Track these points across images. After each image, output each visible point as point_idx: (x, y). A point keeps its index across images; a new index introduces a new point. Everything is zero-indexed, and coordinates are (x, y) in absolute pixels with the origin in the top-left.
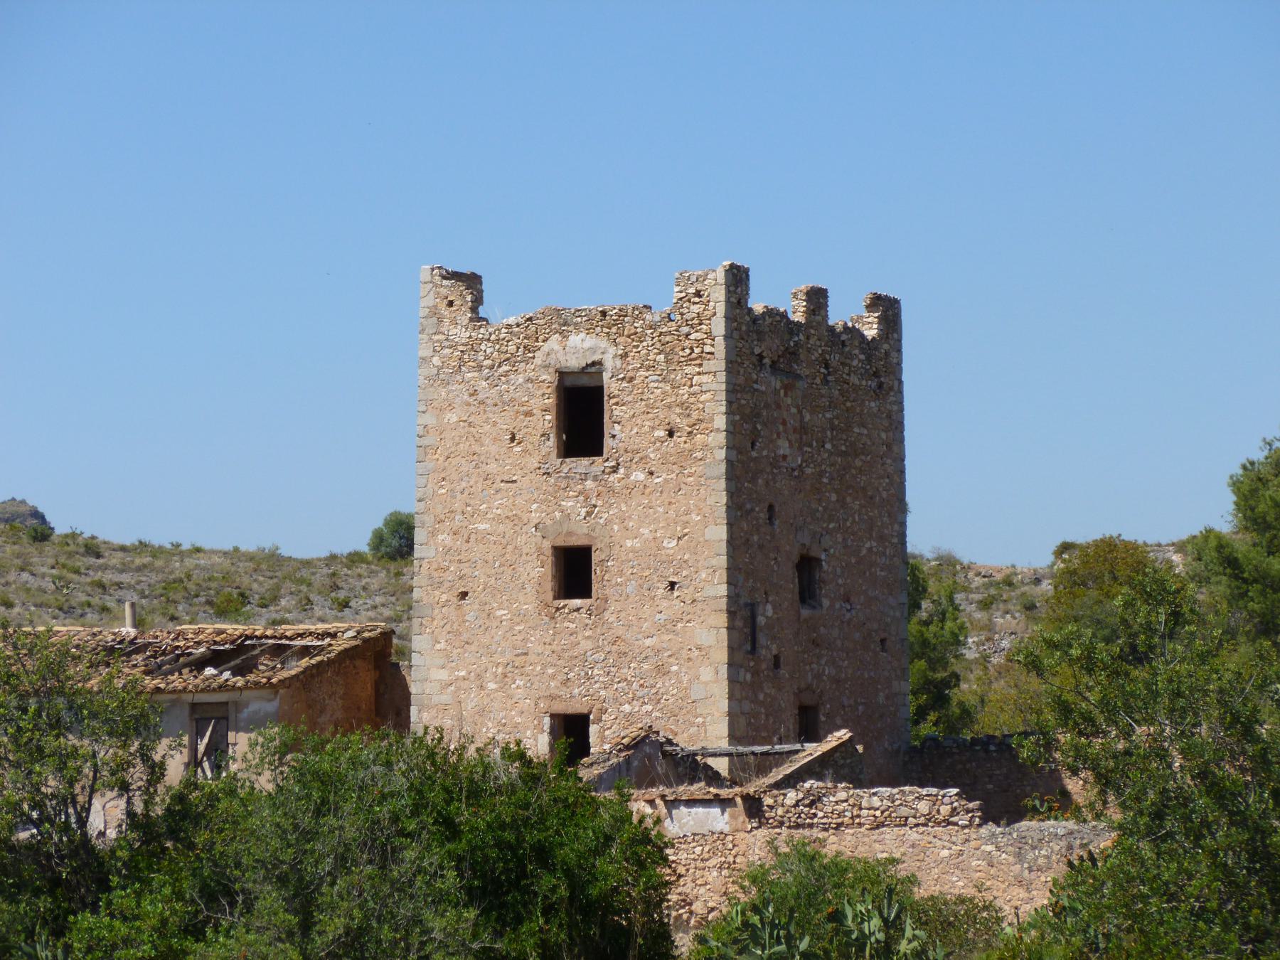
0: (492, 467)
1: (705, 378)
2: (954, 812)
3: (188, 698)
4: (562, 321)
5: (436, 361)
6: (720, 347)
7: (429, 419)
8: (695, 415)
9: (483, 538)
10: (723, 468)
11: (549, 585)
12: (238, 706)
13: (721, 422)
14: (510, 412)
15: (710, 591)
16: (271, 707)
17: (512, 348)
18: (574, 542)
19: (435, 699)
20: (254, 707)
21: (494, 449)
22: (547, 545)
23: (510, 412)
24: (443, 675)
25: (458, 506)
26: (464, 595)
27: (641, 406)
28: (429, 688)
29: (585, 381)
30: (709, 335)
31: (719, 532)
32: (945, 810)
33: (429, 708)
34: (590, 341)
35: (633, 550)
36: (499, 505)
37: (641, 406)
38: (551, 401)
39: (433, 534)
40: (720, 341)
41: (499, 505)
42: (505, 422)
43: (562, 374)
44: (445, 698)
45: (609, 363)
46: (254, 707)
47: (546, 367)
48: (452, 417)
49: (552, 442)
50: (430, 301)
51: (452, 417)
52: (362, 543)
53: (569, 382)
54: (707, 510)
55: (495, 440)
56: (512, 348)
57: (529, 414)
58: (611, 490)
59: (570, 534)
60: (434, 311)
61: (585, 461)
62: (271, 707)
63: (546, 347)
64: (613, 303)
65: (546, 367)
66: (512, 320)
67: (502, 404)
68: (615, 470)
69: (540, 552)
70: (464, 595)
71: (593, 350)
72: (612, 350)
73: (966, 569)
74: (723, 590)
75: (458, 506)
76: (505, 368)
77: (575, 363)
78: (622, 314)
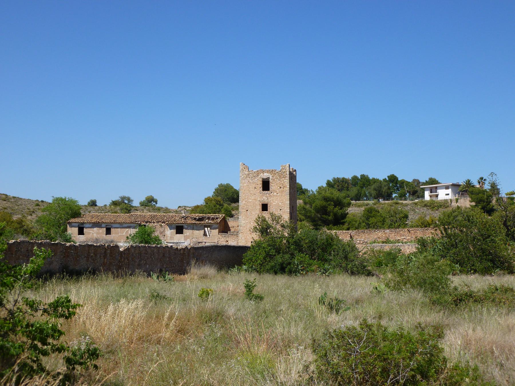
0: (252, 192)
1: (286, 180)
2: (363, 242)
3: (204, 225)
4: (263, 172)
5: (243, 176)
6: (288, 175)
7: (241, 185)
8: (284, 185)
9: (250, 202)
10: (289, 193)
11: (261, 209)
12: (212, 226)
13: (288, 186)
14: (255, 184)
15: (287, 211)
16: (217, 226)
17: (255, 175)
18: (265, 203)
19: (243, 226)
20: (214, 226)
21: (252, 189)
22: (261, 203)
23: (255, 184)
24: (244, 222)
25: (246, 197)
26: (247, 210)
27: (276, 184)
28: (241, 224)
29: (266, 180)
30: (286, 174)
31: (288, 202)
32: (362, 242)
33: (242, 227)
34: (268, 174)
35: (274, 204)
36: (253, 197)
37: (276, 184)
38: (261, 183)
39: (242, 201)
40: (288, 175)
41: (253, 197)
42: (254, 186)
43: (263, 179)
44: (244, 225)
45: (271, 177)
46: (214, 226)
47: (260, 178)
48: (245, 185)
49: (261, 188)
50: (242, 168)
51: (245, 185)
52: (86, 204)
53: (264, 180)
54: (286, 199)
55: (252, 188)
56: (255, 175)
57: (258, 184)
58: (271, 196)
59: (264, 202)
60: (242, 169)
61: (267, 192)
62: (217, 226)
63: (260, 175)
64: (271, 169)
65: (260, 178)
66: (255, 171)
67: (253, 183)
68: (271, 193)
69: (260, 205)
70: (247, 210)
71: (268, 176)
72: (271, 176)
73: (170, 209)
74: (289, 210)
75: (246, 197)
76: (254, 178)
77: (265, 177)
78: (273, 171)
